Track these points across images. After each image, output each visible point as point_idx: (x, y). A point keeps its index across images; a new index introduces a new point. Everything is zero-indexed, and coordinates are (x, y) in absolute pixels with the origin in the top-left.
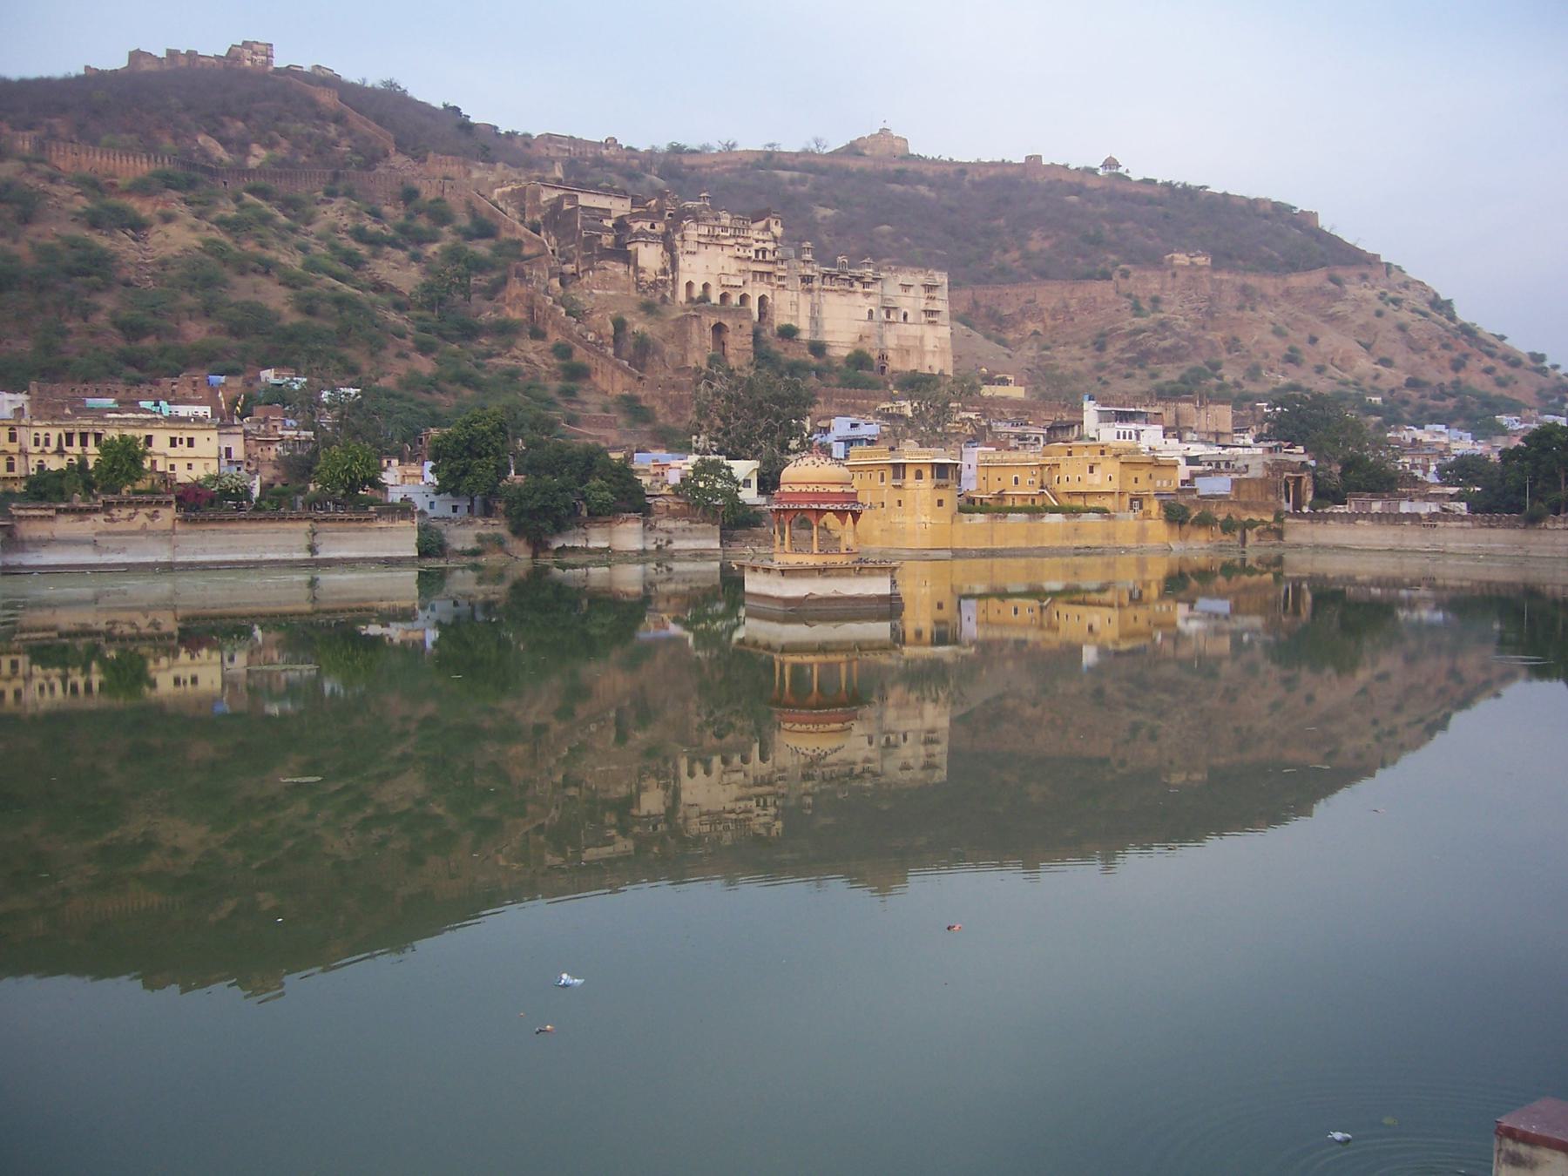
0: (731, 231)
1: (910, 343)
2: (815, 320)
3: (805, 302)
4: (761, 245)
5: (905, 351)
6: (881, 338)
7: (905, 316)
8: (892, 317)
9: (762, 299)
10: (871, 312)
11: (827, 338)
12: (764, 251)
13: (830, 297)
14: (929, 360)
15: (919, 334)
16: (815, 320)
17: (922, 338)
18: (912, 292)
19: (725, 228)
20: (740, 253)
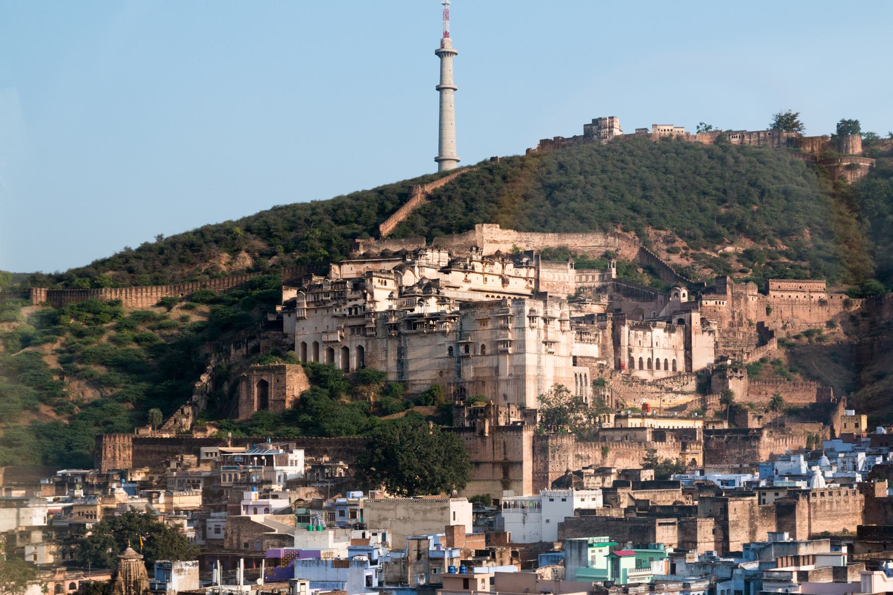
0: (332, 295)
1: (487, 374)
2: (401, 363)
3: (392, 346)
4: (353, 303)
5: (479, 382)
6: (459, 373)
7: (483, 347)
8: (471, 353)
9: (360, 349)
10: (450, 349)
11: (411, 378)
12: (356, 307)
13: (414, 341)
14: (503, 388)
15: (495, 365)
16: (401, 363)
17: (497, 369)
18: (490, 326)
19: (327, 294)
20: (337, 312)
